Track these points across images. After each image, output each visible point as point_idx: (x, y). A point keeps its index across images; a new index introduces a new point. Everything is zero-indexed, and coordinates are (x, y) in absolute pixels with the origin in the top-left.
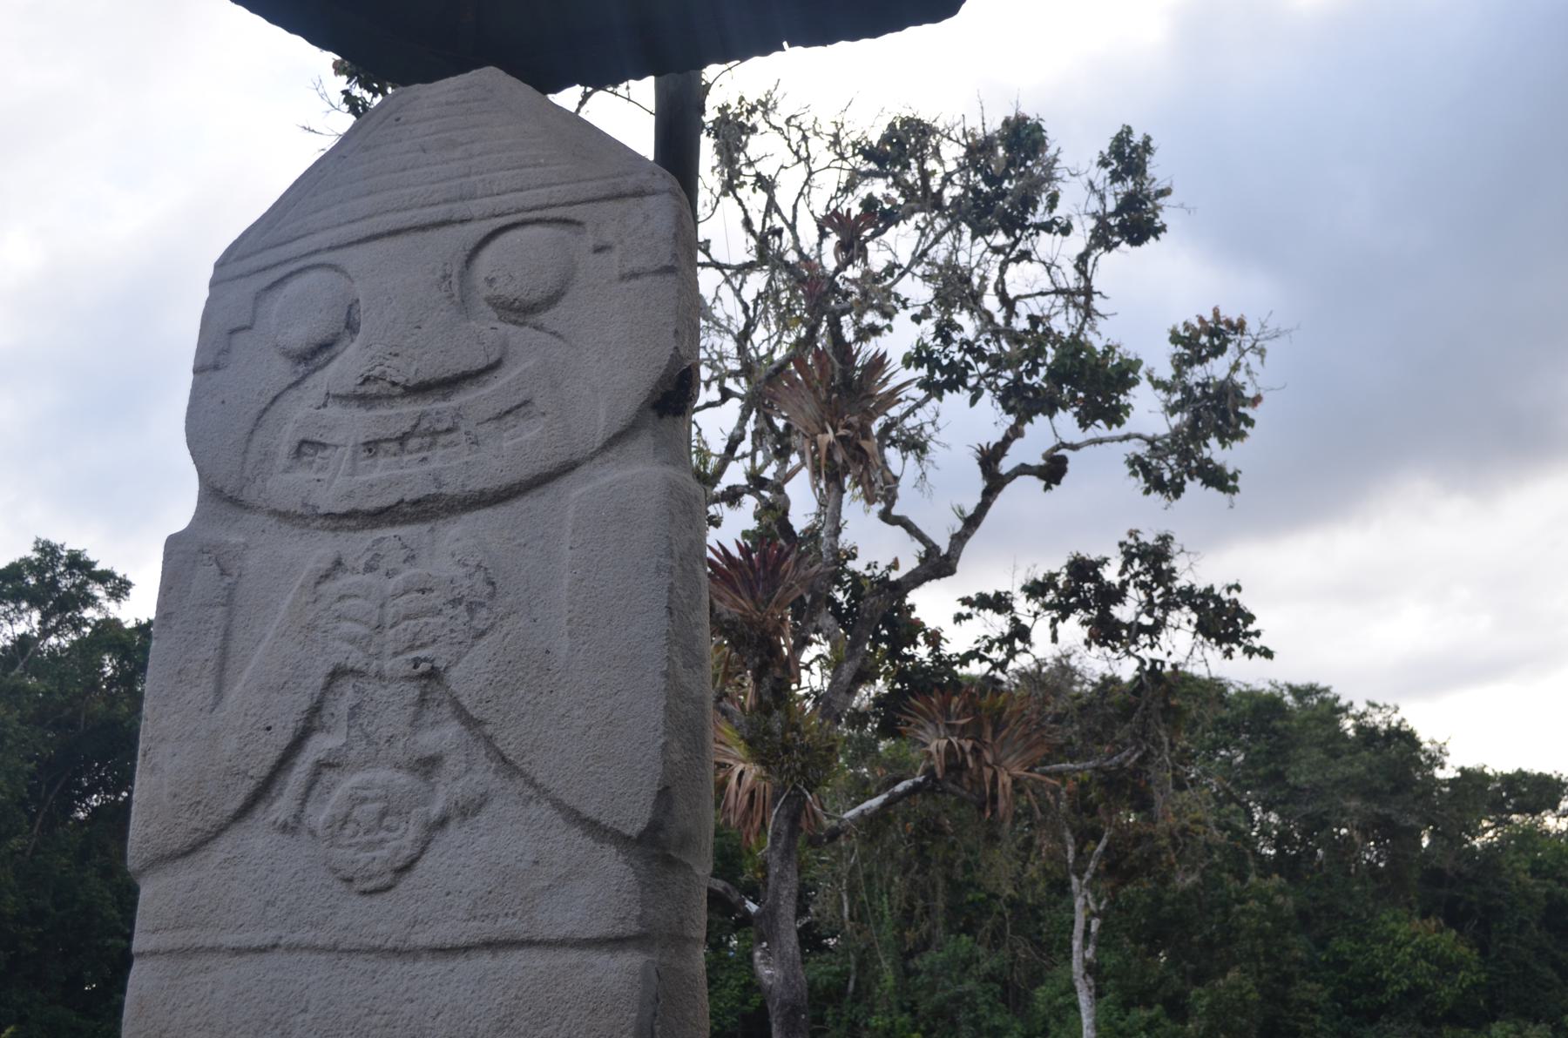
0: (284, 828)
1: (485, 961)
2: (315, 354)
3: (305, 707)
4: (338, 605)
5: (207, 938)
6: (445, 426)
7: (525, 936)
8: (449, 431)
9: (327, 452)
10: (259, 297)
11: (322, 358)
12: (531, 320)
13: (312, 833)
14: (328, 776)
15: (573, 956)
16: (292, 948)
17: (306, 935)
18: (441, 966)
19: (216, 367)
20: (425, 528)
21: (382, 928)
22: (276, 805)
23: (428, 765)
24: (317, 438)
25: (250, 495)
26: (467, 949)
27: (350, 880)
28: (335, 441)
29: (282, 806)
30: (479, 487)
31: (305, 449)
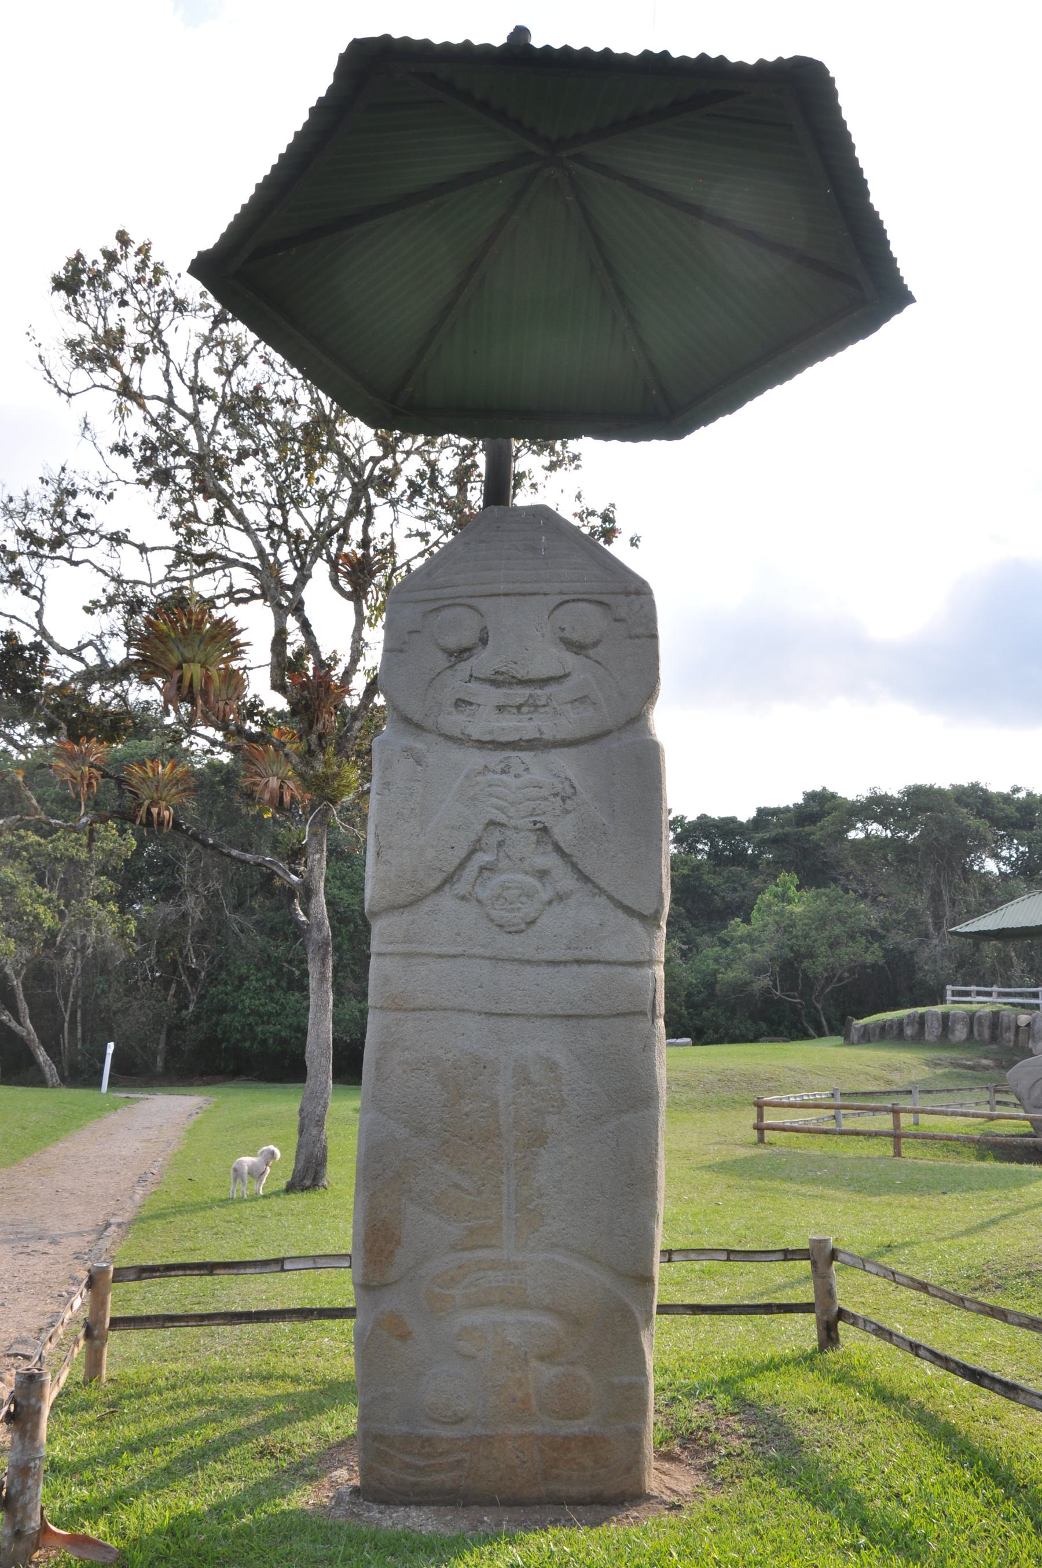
0: (463, 898)
1: (575, 968)
2: (462, 653)
3: (473, 839)
4: (488, 789)
5: (425, 949)
6: (543, 703)
7: (595, 958)
8: (544, 706)
9: (473, 707)
10: (425, 614)
11: (465, 655)
12: (584, 652)
13: (479, 901)
14: (486, 874)
15: (620, 969)
16: (470, 957)
17: (481, 951)
18: (551, 970)
19: (401, 651)
20: (532, 754)
21: (520, 950)
22: (456, 886)
23: (542, 874)
24: (467, 699)
25: (428, 723)
26: (565, 963)
27: (501, 926)
28: (479, 702)
29: (461, 887)
30: (563, 737)
31: (460, 703)
